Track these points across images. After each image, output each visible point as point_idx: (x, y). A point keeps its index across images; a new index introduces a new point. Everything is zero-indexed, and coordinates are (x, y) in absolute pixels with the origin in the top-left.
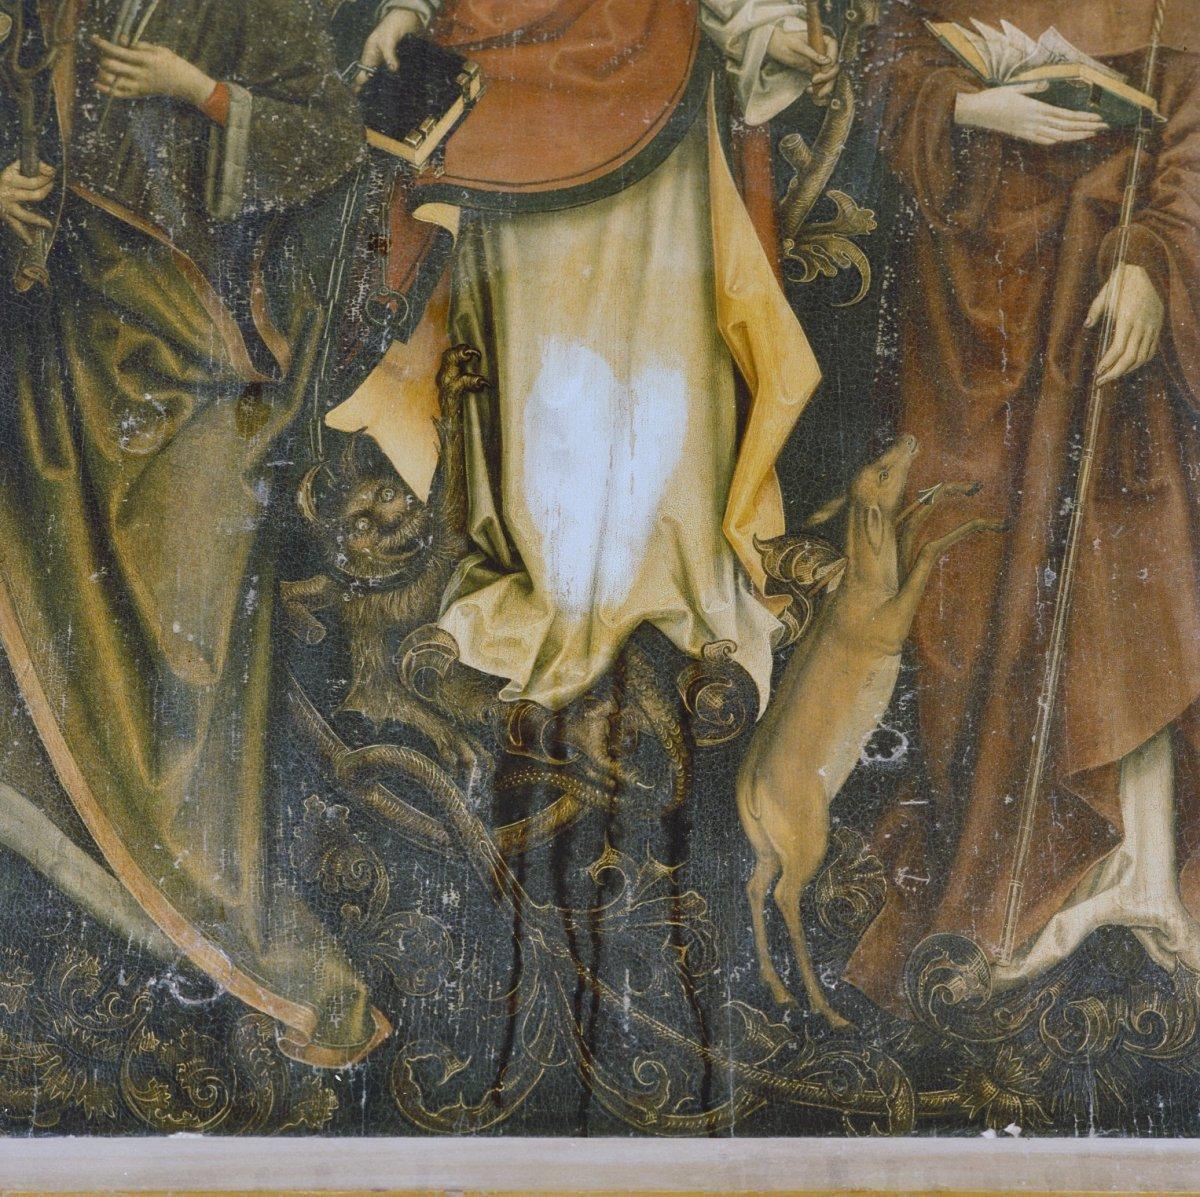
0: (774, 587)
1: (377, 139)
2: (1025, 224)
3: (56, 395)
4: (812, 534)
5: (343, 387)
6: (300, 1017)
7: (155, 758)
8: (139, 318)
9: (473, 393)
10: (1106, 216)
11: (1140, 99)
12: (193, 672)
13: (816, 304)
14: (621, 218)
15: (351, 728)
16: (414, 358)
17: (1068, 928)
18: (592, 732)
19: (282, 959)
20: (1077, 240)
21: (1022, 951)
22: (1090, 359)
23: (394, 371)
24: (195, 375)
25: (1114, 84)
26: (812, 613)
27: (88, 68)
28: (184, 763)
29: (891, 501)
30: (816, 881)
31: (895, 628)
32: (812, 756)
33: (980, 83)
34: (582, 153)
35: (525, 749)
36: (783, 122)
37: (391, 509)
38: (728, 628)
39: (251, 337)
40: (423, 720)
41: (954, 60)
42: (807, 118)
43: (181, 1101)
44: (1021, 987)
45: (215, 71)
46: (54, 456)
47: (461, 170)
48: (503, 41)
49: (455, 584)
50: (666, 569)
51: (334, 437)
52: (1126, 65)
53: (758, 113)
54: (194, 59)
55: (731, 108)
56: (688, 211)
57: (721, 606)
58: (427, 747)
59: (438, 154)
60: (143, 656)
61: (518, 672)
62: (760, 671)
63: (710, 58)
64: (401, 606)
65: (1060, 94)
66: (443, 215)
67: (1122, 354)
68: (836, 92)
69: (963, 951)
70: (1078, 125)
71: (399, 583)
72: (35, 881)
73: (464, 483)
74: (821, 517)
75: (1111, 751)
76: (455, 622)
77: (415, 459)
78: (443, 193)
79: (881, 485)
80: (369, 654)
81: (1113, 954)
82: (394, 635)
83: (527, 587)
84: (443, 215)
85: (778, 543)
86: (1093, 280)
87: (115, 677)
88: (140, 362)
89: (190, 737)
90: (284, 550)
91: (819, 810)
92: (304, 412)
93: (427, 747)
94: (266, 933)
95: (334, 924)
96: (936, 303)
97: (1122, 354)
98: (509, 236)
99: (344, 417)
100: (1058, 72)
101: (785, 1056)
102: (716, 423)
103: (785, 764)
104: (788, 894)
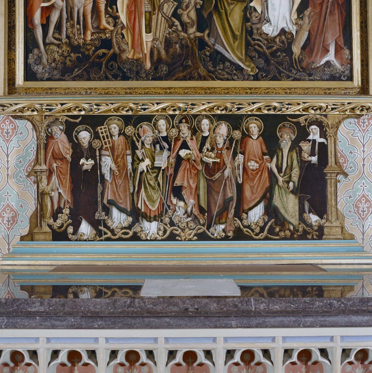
0: (296, 24)
3: (222, 2)
4: (300, 18)
6: (249, 69)
7: (234, 42)
15: (254, 40)
18: (277, 40)
19: (247, 63)
26: (300, 28)
28: (237, 43)
29: (308, 14)
30: (300, 55)
31: (308, 29)
32: (299, 43)
38: (291, 29)
40: (260, 38)
43: (238, 78)
46: (222, 9)
49: (263, 24)
50: (285, 22)
51: (251, 7)
57: (290, 26)
58: (261, 41)
62: (294, 33)
64: (258, 26)
71: (258, 23)
72: (223, 56)
74: (301, 16)
75: (329, 42)
79: (307, 13)
80: (255, 31)
81: (328, 63)
83: (271, 24)
85: (296, 19)
89: (237, 40)
90: (246, 19)
92: (248, 4)
93: (261, 41)
94: (246, 61)
95: (252, 60)
101: (296, 73)
102: (290, 5)
103: (297, 43)
104: (297, 57)
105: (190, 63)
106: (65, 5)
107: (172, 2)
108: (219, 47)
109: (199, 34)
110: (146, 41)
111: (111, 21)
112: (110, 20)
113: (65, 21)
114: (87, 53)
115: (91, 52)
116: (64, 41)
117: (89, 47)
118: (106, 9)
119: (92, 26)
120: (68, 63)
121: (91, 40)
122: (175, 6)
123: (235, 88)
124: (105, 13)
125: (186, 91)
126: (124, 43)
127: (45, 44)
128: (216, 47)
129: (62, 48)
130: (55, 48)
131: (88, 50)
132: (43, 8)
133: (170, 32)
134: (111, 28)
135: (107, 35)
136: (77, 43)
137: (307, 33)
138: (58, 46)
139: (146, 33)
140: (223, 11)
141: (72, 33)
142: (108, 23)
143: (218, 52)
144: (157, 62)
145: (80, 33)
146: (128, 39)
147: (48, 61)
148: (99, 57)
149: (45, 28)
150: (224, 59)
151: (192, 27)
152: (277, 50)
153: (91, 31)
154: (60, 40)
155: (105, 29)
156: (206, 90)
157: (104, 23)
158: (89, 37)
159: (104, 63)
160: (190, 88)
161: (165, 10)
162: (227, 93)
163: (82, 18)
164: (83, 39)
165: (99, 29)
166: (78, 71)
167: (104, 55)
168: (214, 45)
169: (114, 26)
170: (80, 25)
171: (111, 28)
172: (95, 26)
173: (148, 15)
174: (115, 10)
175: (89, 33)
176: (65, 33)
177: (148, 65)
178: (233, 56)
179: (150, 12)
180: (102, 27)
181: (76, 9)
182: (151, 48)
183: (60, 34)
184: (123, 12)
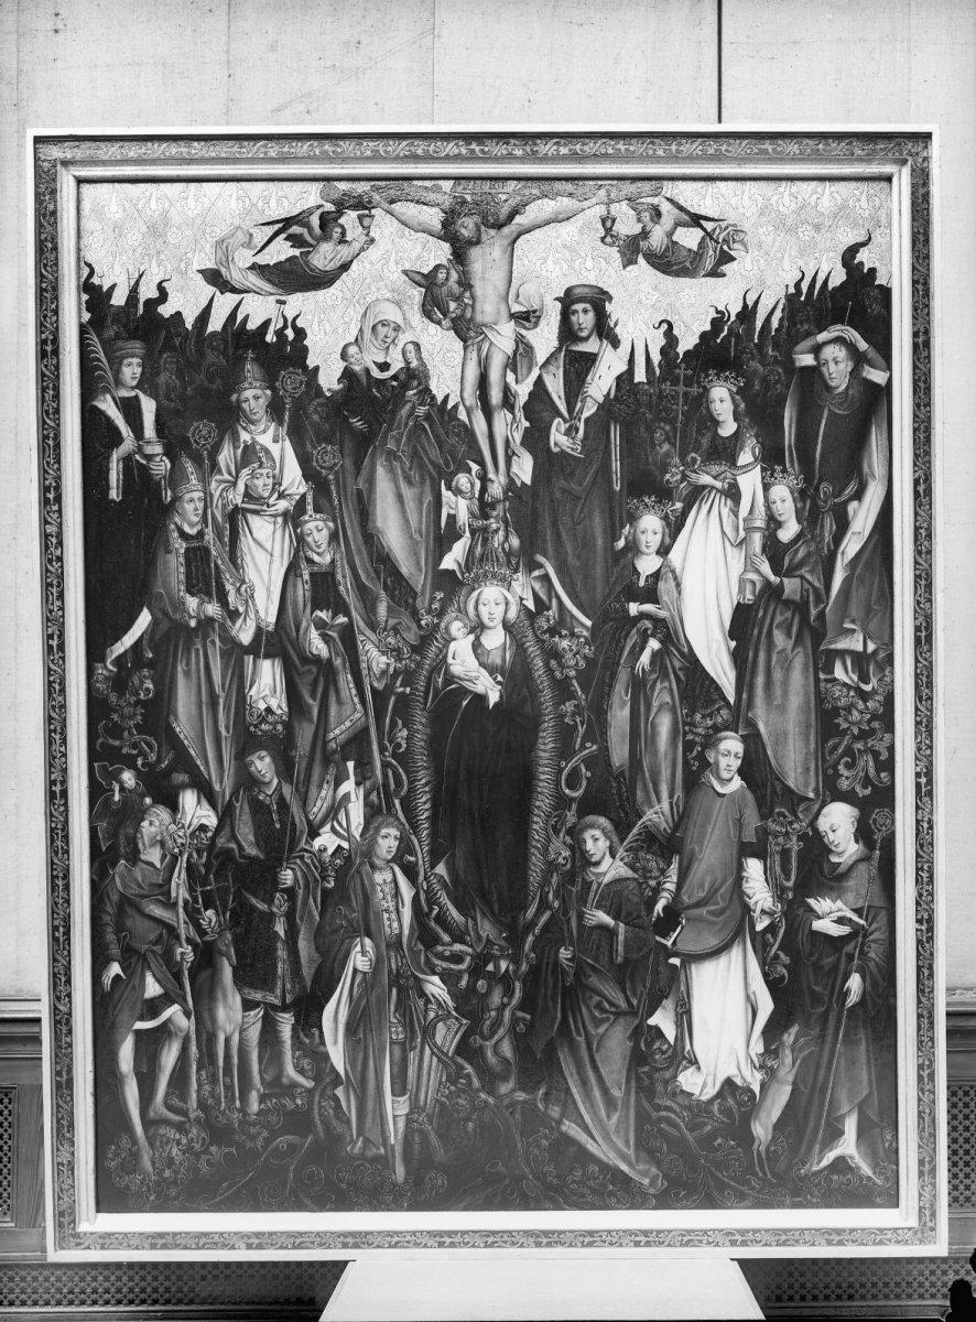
0: (761, 1067)
1: (658, 938)
2: (828, 961)
5: (651, 1014)
6: (646, 1181)
7: (609, 1117)
8: (599, 993)
9: (684, 1016)
10: (850, 957)
11: (862, 922)
12: (617, 1093)
13: (773, 985)
14: (723, 959)
15: (658, 1108)
16: (669, 1003)
17: (830, 1157)
18: (716, 1107)
20: (842, 966)
21: (820, 1162)
22: (845, 1000)
23: (664, 1008)
24: (613, 1009)
25: (855, 918)
26: (770, 1074)
27: (581, 916)
28: (615, 1117)
31: (791, 1078)
32: (769, 1115)
33: (819, 917)
34: (713, 942)
35: (699, 1110)
36: (766, 930)
37: (665, 1047)
38: (749, 1079)
39: (628, 1001)
41: (812, 910)
42: (772, 929)
44: (820, 1172)
45: (616, 917)
46: (579, 1034)
47: (680, 947)
48: (689, 907)
50: (734, 1064)
51: (649, 1026)
52: (858, 911)
53: (759, 927)
54: (608, 914)
55: (752, 926)
56: (740, 958)
58: (675, 1112)
59: (674, 943)
60: (605, 1091)
61: (697, 1092)
62: (756, 1088)
63: (747, 910)
64: (667, 1075)
65: (841, 921)
66: (675, 961)
67: (853, 999)
68: (780, 921)
69: (804, 1163)
70: (844, 930)
71: (668, 1068)
72: (582, 1150)
73: (683, 1040)
76: (682, 1078)
77: (670, 1032)
78: (676, 955)
79: (789, 1038)
80: (659, 1088)
81: (841, 1160)
82: (666, 1082)
83: (699, 1068)
84: (675, 961)
85: (762, 1055)
86: (846, 977)
87: (597, 1093)
88: (599, 1006)
89: (616, 1110)
90: (638, 1058)
91: (771, 1127)
93: (675, 1112)
95: (653, 1158)
96: (805, 985)
97: (853, 999)
98: (693, 967)
99: (652, 1021)
100: (840, 914)
103: (763, 1115)
104: (762, 1148)
105: (501, 1167)
106: (193, 1028)
107: (457, 1019)
108: (571, 1129)
109: (521, 1096)
110: (395, 1117)
111: (307, 1067)
112: (306, 1063)
113: (194, 1068)
114: (249, 1144)
115: (260, 1143)
116: (192, 1116)
117: (253, 1130)
118: (295, 1036)
119: (262, 1078)
120: (204, 1169)
121: (260, 1113)
122: (463, 1029)
123: (609, 1232)
124: (293, 1045)
125: (490, 1240)
126: (338, 1118)
127: (146, 1123)
128: (564, 1128)
129: (187, 1132)
130: (172, 1134)
131: (253, 1138)
132: (138, 1033)
133: (451, 1093)
134: (309, 1084)
135: (299, 1102)
136: (224, 1121)
137: (788, 1089)
138: (180, 1128)
139: (393, 1094)
140: (581, 1039)
141: (213, 1097)
142: (301, 1071)
143: (568, 1140)
144: (419, 1162)
145: (233, 1096)
146: (350, 1111)
147: (153, 1163)
148: (277, 1153)
149: (147, 1082)
150: (584, 1156)
151: (506, 1079)
152: (712, 1136)
153: (258, 1090)
154: (184, 1113)
155: (295, 1085)
156: (538, 1236)
157: (290, 1070)
158: (254, 1107)
159: (292, 1168)
160: (498, 1232)
161: (439, 1039)
162: (590, 1244)
163: (235, 1060)
164: (240, 1111)
165: (277, 1087)
166: (229, 1188)
167: (293, 1148)
168: (559, 1122)
169: (317, 1078)
170: (232, 1078)
171: (309, 1084)
172: (268, 1078)
173: (397, 1050)
174: (317, 1040)
175: (254, 1096)
176: (194, 1095)
177: (400, 1171)
178: (605, 1147)
179: (403, 1044)
180: (285, 1080)
181: (222, 1038)
182: (406, 1136)
183: (184, 1097)
184: (336, 1042)
